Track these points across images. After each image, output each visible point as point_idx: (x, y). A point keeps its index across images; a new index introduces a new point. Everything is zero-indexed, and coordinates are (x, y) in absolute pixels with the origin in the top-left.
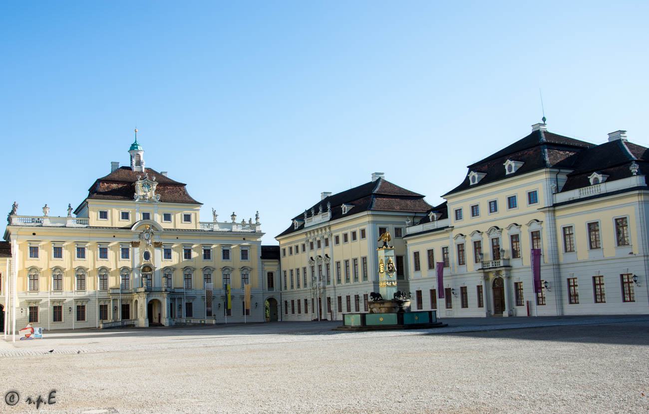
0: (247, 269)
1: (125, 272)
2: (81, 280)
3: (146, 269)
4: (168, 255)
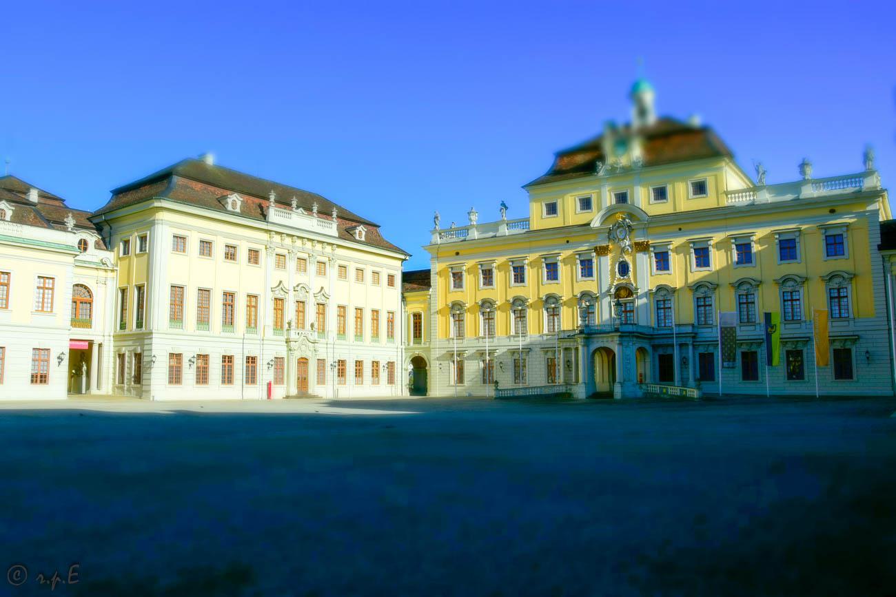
0: (795, 281)
1: (587, 301)
2: (489, 319)
3: (623, 293)
4: (663, 261)
